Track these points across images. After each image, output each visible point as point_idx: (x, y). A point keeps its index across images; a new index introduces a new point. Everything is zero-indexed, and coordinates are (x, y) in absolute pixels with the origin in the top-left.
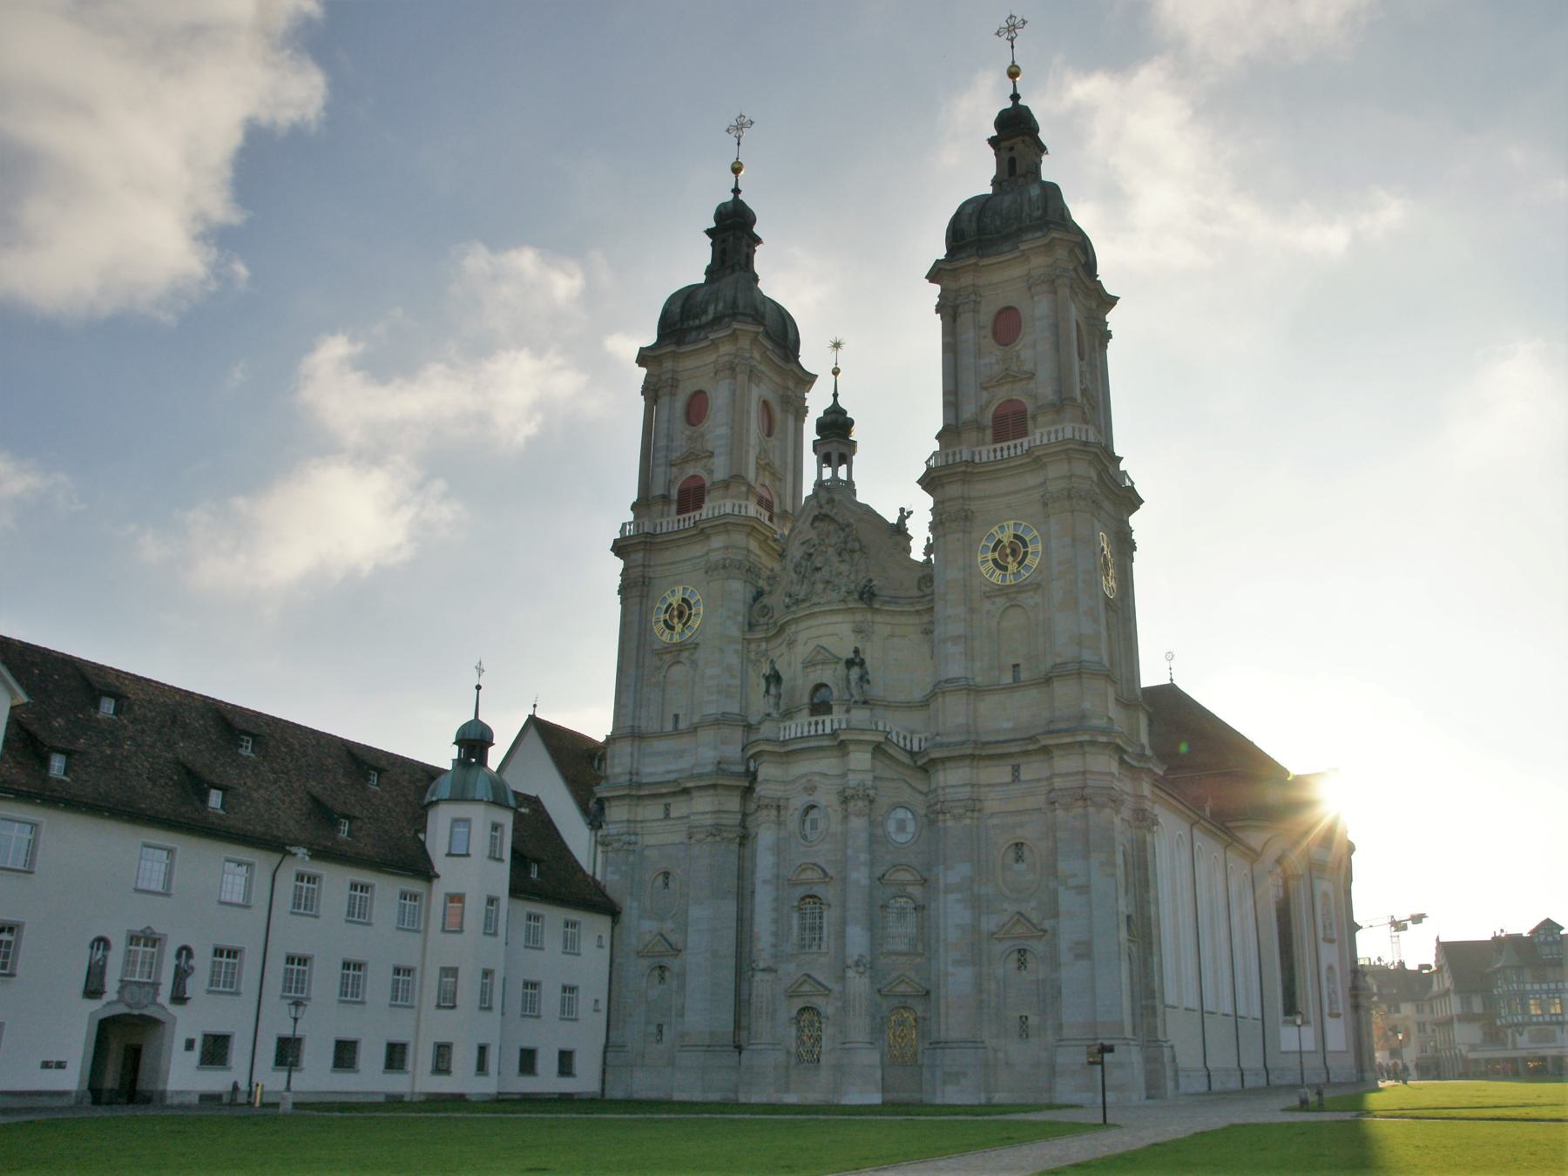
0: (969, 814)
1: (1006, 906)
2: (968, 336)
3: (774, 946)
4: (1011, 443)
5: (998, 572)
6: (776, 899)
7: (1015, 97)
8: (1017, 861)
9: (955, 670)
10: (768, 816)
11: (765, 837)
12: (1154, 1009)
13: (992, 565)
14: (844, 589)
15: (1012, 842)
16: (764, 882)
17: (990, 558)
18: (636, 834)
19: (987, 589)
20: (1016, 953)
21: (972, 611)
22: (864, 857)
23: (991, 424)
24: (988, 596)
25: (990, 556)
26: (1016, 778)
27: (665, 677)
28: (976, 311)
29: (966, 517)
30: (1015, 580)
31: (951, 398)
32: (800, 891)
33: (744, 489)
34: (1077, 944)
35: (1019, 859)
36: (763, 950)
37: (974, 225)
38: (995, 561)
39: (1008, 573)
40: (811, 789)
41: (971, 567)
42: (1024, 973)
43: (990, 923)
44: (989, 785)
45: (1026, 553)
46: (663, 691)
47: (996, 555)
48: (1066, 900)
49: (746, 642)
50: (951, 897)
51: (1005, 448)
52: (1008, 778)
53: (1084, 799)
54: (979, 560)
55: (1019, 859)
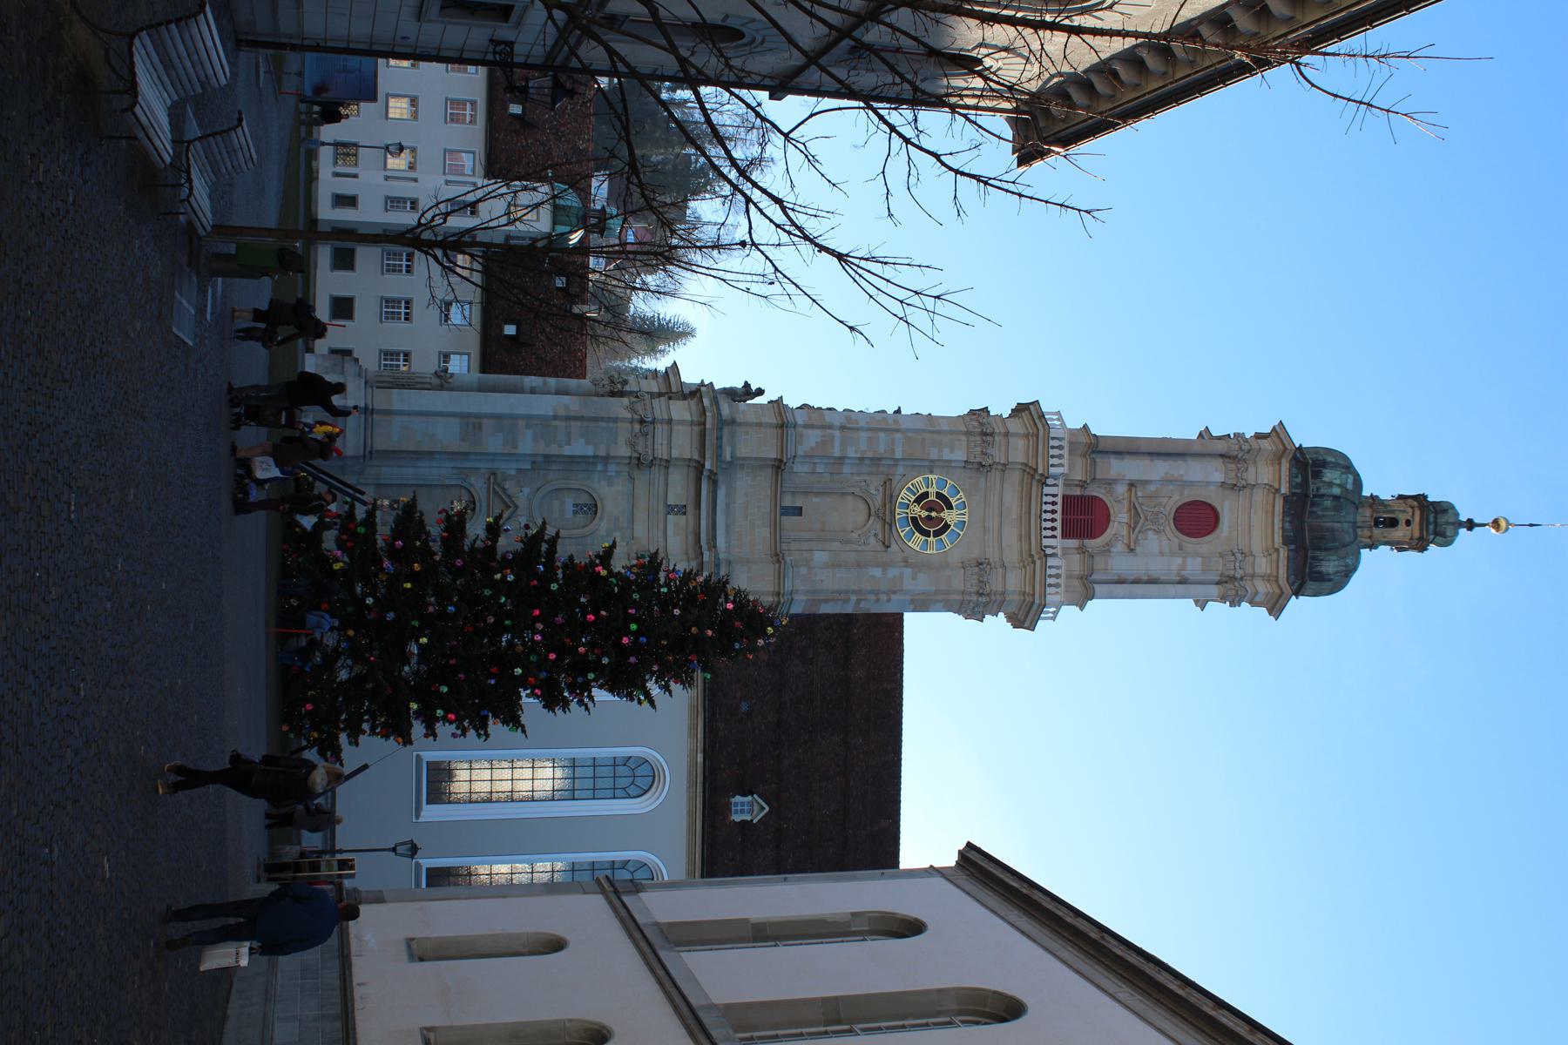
1: (526, 490)
4: (1058, 516)
7: (1470, 525)
13: (920, 492)
17: (930, 490)
19: (894, 482)
24: (887, 483)
25: (933, 490)
26: (670, 509)
30: (899, 519)
38: (926, 495)
45: (927, 534)
47: (932, 498)
51: (1055, 508)
54: (930, 476)
55: (578, 508)
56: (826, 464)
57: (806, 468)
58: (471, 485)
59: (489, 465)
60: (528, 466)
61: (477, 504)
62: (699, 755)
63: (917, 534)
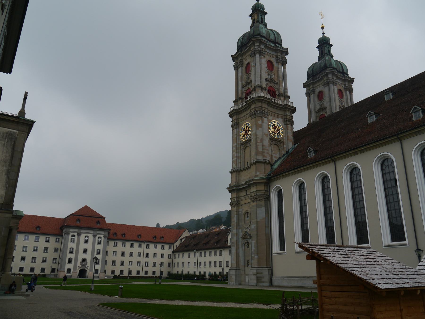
1: (244, 230)
8: (247, 217)
15: (247, 211)
26: (246, 194)
35: (248, 216)
52: (245, 194)
53: (256, 198)
56: (238, 160)
57: (240, 164)
58: (244, 243)
59: (240, 239)
60: (240, 230)
61: (246, 242)
62: (291, 172)
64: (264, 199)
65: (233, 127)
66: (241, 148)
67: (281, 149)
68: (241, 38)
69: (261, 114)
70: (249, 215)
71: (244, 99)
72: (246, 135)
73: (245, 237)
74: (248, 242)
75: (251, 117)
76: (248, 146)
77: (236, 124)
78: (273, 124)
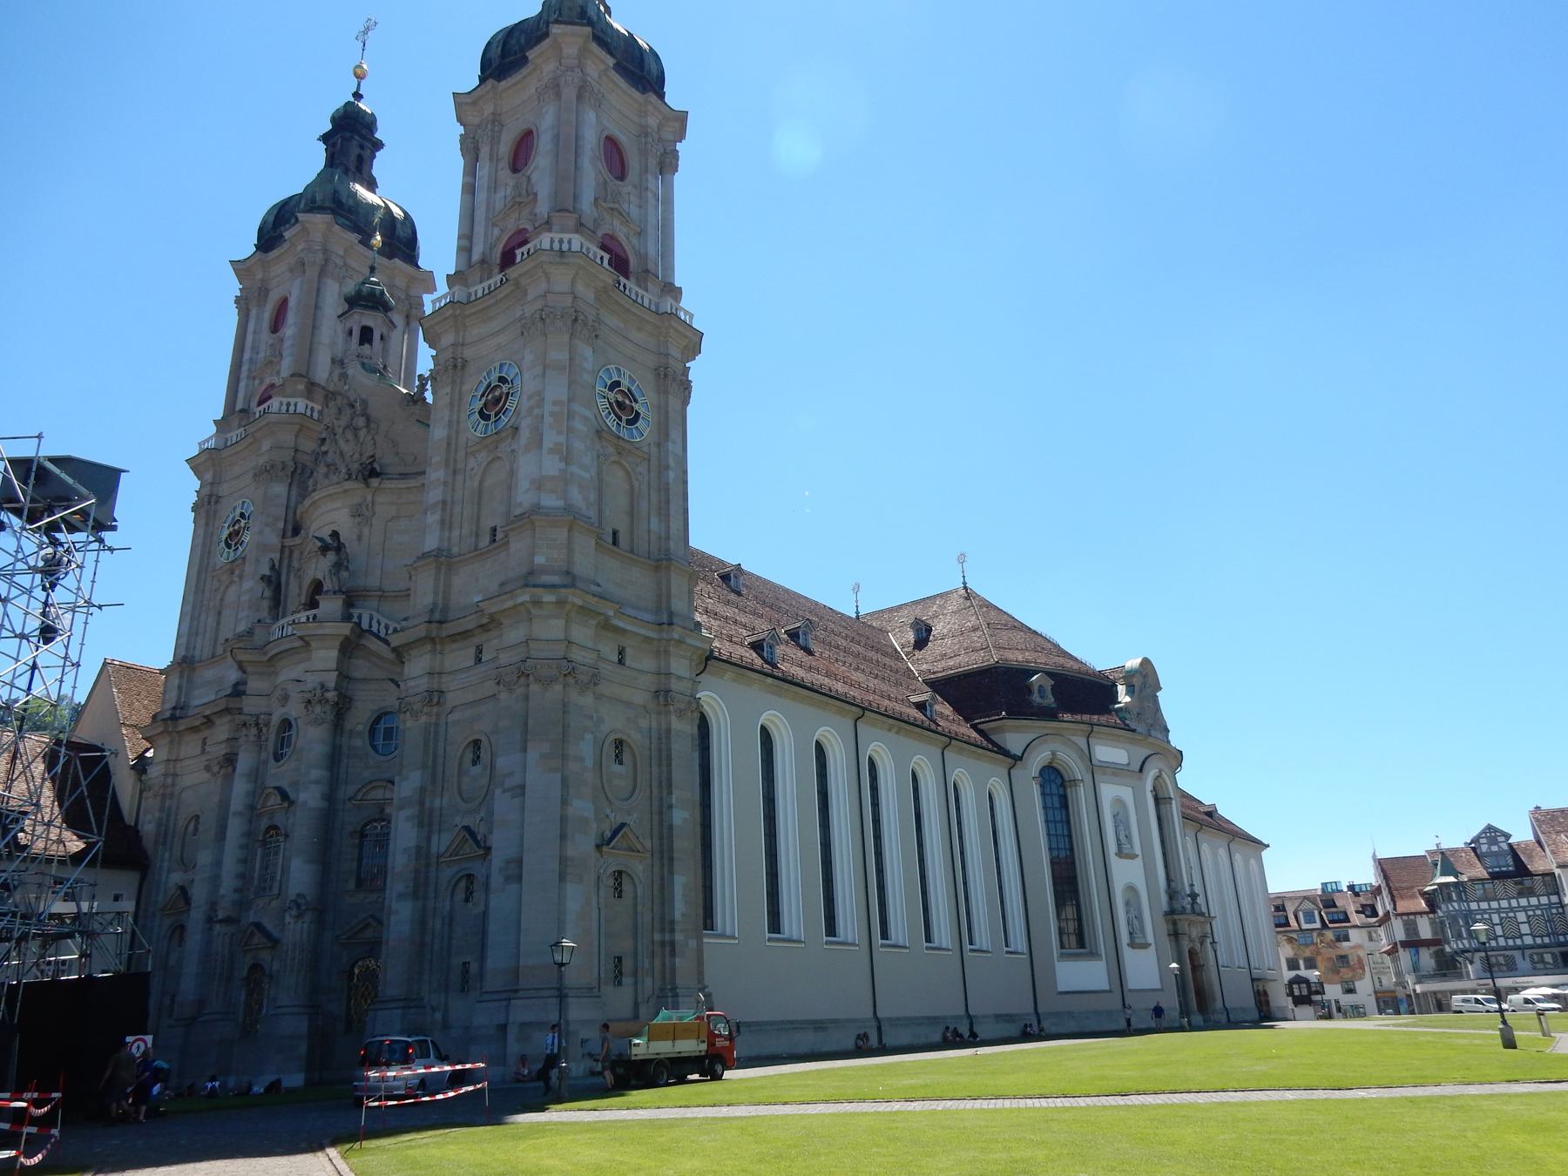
0: (425, 709)
2: (483, 170)
3: (236, 890)
5: (483, 422)
6: (249, 834)
8: (474, 763)
9: (431, 542)
10: (246, 735)
11: (245, 762)
12: (672, 944)
13: (478, 417)
14: (344, 471)
15: (471, 739)
16: (234, 814)
18: (175, 775)
20: (465, 878)
21: (455, 472)
22: (316, 773)
23: (498, 261)
26: (478, 660)
27: (222, 600)
28: (495, 141)
29: (455, 366)
31: (465, 243)
32: (264, 824)
33: (301, 387)
34: (508, 862)
35: (476, 760)
36: (223, 896)
37: (500, 49)
39: (490, 422)
40: (285, 699)
41: (458, 422)
42: (470, 904)
43: (441, 842)
44: (450, 673)
46: (220, 613)
48: (502, 803)
49: (287, 552)
50: (404, 813)
52: (472, 663)
61: (464, 873)
63: (506, 406)
64: (562, 678)
65: (438, 379)
66: (469, 466)
67: (636, 484)
68: (500, 36)
69: (569, 323)
70: (485, 755)
71: (497, 270)
72: (493, 413)
73: (456, 855)
74: (470, 877)
75: (525, 333)
76: (499, 458)
77: (455, 366)
78: (615, 378)
